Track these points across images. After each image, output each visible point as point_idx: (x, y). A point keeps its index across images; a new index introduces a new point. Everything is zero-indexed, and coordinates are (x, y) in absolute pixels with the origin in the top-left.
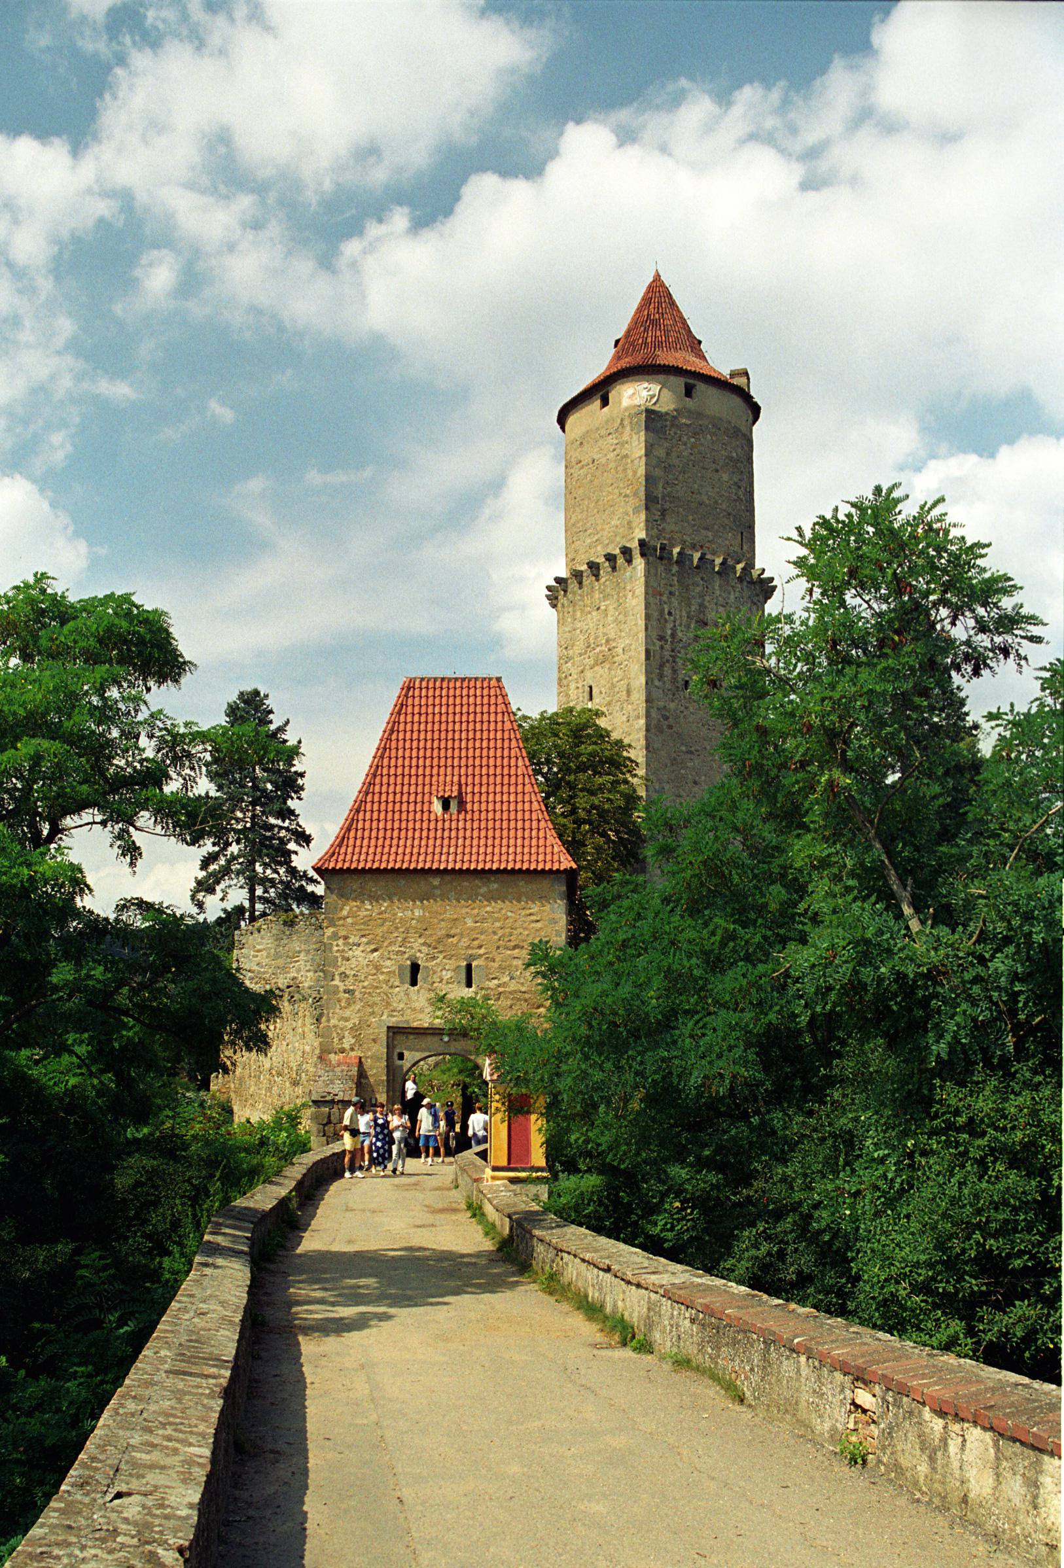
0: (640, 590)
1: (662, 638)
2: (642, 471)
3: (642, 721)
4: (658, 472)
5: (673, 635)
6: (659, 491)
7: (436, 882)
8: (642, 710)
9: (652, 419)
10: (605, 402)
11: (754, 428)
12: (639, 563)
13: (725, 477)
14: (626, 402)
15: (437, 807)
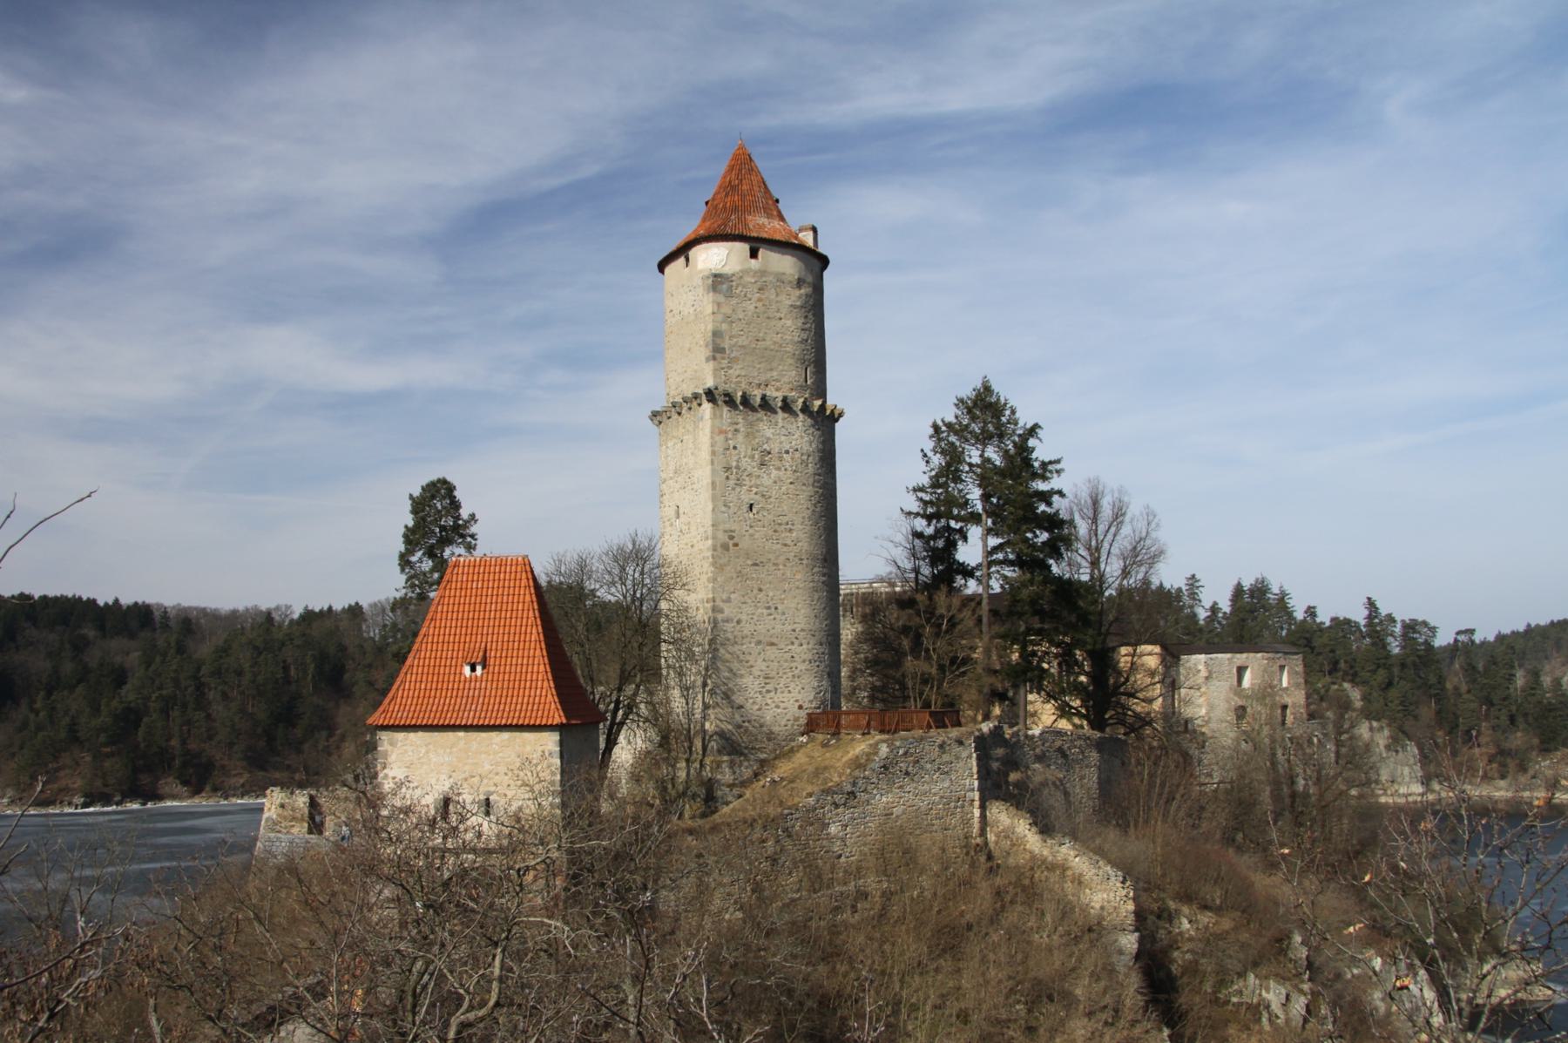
0: (708, 431)
1: (728, 469)
2: (710, 327)
3: (710, 542)
4: (724, 326)
5: (738, 467)
6: (726, 344)
7: (461, 734)
8: (710, 531)
9: (718, 281)
10: (687, 260)
11: (825, 273)
12: (707, 406)
13: (789, 323)
14: (700, 266)
15: (467, 670)
